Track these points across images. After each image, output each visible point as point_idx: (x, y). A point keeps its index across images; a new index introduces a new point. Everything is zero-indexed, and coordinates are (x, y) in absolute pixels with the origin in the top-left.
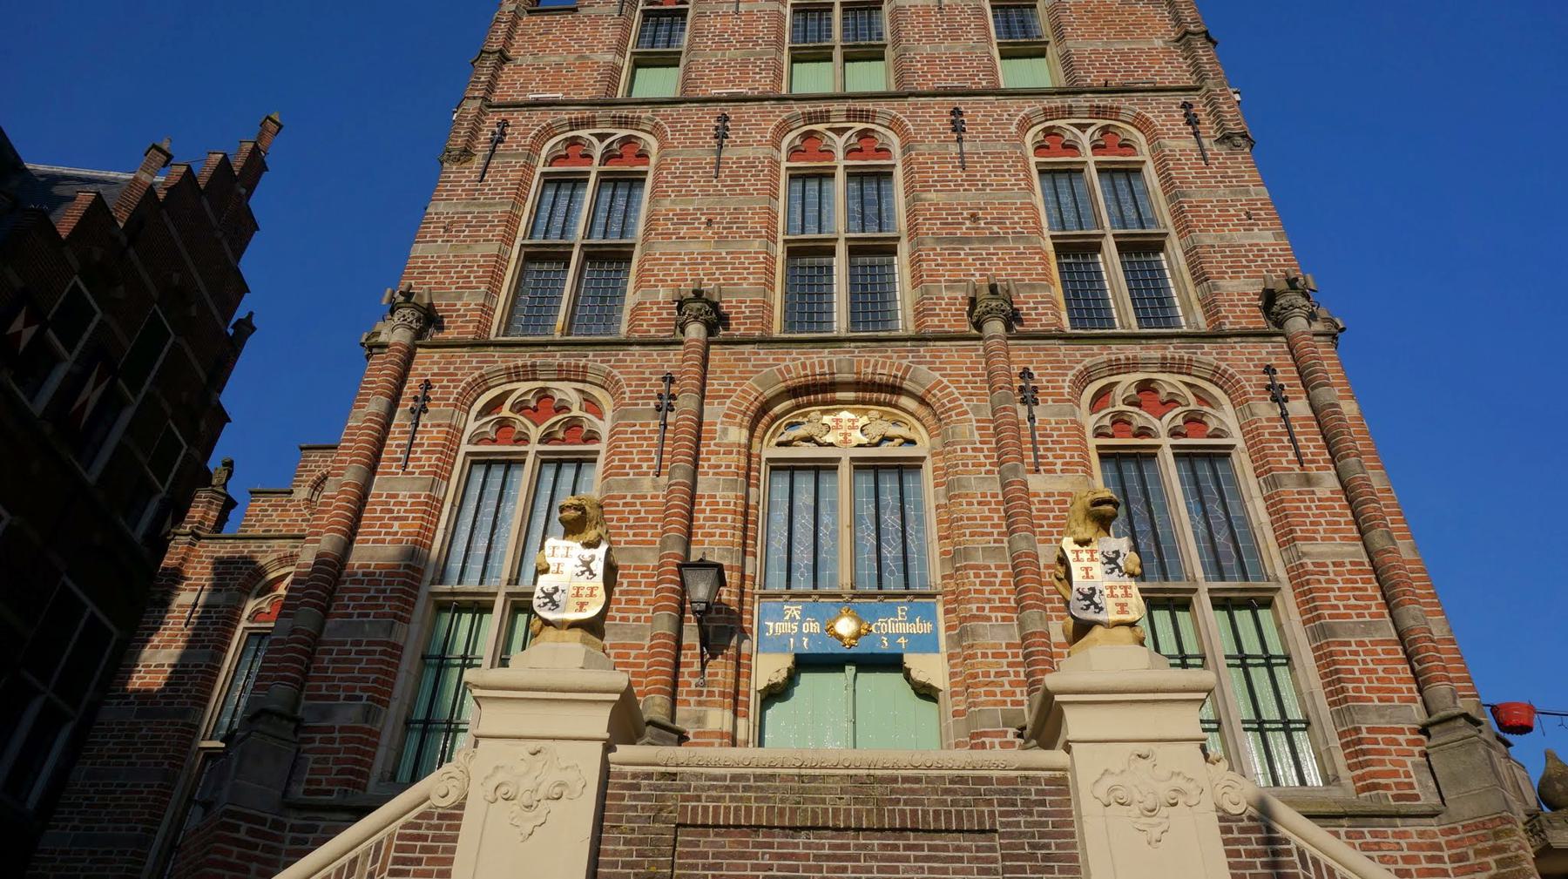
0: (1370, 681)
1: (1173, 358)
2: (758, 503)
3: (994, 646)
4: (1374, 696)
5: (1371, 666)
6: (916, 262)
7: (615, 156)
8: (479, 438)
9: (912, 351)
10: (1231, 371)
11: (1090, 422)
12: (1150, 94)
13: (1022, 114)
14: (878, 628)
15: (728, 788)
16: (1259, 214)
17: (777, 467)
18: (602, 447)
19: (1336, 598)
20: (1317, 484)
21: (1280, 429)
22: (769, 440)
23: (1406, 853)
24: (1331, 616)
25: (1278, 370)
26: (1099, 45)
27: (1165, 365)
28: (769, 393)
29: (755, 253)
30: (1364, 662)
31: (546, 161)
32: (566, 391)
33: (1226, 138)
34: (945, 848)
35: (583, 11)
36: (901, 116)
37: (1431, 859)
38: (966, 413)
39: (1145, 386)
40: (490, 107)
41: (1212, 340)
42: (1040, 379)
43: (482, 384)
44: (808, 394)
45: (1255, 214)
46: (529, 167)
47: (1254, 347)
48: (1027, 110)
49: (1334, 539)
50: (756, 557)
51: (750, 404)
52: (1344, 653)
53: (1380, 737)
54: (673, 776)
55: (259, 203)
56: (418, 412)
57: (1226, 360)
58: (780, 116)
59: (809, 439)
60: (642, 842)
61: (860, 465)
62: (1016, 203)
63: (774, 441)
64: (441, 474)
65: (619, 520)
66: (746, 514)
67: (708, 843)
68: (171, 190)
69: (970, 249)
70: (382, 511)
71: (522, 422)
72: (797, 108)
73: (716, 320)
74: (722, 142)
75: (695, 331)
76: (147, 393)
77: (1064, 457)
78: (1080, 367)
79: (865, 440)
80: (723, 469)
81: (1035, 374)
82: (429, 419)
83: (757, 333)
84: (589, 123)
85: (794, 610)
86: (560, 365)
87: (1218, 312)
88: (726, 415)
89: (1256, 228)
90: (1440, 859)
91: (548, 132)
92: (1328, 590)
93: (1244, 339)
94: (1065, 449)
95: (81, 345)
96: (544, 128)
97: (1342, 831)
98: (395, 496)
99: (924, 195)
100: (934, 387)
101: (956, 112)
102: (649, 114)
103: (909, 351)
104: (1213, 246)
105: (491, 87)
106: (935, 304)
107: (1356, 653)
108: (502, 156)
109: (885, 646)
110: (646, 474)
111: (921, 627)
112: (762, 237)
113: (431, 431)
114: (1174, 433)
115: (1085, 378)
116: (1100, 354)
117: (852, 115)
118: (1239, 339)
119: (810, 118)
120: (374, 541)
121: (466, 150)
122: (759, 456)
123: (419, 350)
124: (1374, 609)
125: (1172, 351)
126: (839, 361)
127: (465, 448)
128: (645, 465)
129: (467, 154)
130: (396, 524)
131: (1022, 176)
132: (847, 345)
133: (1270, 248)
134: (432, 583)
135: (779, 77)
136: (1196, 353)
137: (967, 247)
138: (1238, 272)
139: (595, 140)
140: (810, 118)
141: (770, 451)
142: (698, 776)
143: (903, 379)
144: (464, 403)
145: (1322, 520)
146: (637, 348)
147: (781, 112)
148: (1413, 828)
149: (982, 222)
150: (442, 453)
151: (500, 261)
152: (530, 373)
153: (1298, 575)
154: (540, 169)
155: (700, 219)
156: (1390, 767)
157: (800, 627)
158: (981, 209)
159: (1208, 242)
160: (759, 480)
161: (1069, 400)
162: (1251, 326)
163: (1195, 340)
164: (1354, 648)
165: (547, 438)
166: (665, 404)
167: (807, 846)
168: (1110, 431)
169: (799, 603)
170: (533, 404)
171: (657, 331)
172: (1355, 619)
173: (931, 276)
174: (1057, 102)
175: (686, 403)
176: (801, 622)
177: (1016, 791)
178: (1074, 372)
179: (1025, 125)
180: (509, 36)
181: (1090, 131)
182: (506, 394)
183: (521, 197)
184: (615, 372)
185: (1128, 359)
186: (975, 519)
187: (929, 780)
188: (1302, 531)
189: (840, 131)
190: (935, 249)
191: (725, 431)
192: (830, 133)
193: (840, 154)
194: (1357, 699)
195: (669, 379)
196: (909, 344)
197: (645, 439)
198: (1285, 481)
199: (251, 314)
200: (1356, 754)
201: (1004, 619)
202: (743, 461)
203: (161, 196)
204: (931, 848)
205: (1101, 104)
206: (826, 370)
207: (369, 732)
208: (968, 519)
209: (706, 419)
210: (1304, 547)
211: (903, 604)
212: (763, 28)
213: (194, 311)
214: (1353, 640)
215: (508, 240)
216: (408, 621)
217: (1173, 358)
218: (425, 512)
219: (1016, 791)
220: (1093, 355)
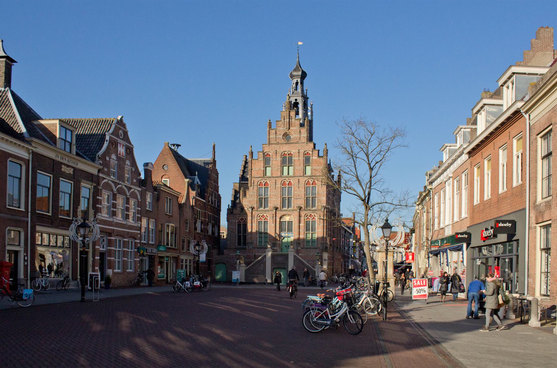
6: (293, 201)
11: (306, 218)
27: (312, 213)
32: (265, 215)
35: (259, 159)
39: (310, 215)
43: (258, 215)
46: (257, 187)
51: (279, 217)
61: (288, 222)
64: (257, 223)
72: (283, 179)
73: (276, 209)
75: (274, 210)
99: (295, 192)
101: (299, 180)
111: (292, 235)
114: (312, 219)
115: (306, 214)
117: (288, 179)
119: (284, 180)
140: (284, 180)
141: (281, 220)
152: (262, 213)
165: (264, 219)
179: (305, 182)
183: (257, 191)
215: (257, 198)
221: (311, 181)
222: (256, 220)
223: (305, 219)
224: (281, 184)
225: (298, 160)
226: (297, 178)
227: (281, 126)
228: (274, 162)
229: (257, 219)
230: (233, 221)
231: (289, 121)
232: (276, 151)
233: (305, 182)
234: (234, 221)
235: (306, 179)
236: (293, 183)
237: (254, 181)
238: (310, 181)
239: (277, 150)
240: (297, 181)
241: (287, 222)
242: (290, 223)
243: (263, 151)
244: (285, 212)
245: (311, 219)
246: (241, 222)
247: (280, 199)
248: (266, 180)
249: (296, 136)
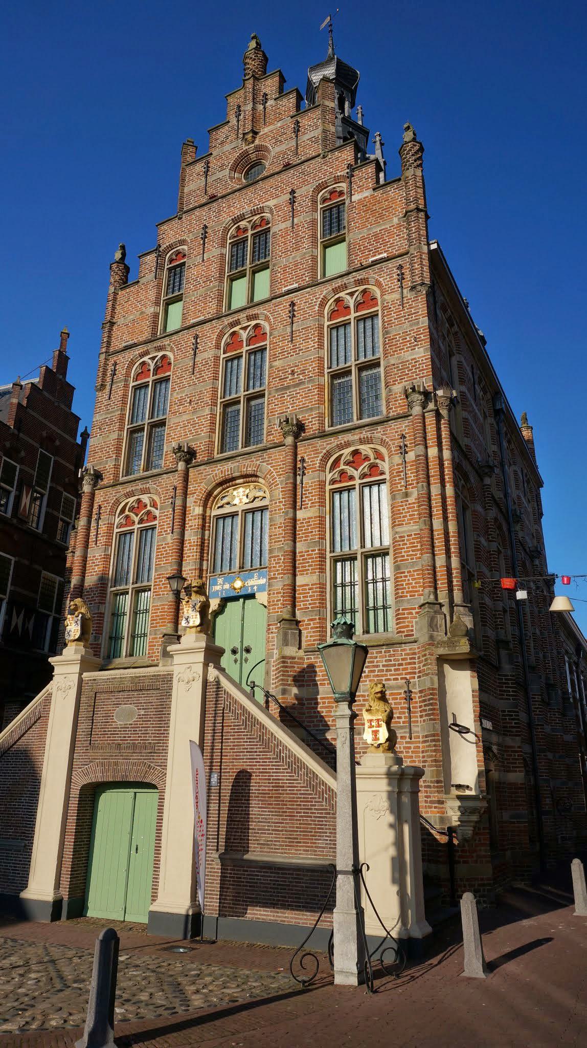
0: (409, 588)
1: (364, 438)
2: (209, 537)
3: (277, 590)
4: (408, 595)
5: (411, 581)
7: (159, 367)
8: (120, 525)
9: (261, 456)
10: (387, 440)
11: (329, 477)
12: (384, 263)
13: (322, 296)
14: (247, 584)
15: (106, 682)
16: (420, 337)
17: (218, 518)
19: (405, 552)
20: (410, 496)
21: (401, 469)
22: (215, 506)
23: (403, 657)
24: (401, 561)
25: (407, 436)
26: (365, 232)
27: (362, 441)
28: (209, 488)
29: (207, 415)
30: (409, 580)
31: (134, 378)
33: (413, 288)
34: (150, 694)
35: (142, 281)
36: (268, 313)
37: (411, 659)
38: (278, 484)
39: (356, 453)
40: (109, 355)
41: (382, 424)
43: (118, 502)
44: (226, 483)
45: (419, 338)
46: (126, 386)
47: (400, 424)
48: (325, 292)
49: (410, 523)
50: (208, 561)
52: (401, 577)
53: (406, 612)
54: (94, 680)
55: (70, 379)
57: (386, 434)
58: (219, 328)
59: (228, 503)
60: (88, 697)
61: (246, 512)
62: (311, 359)
63: (217, 506)
64: (108, 544)
65: (161, 555)
66: (203, 543)
67: (103, 696)
68: (29, 398)
69: (290, 392)
70: (92, 563)
74: (196, 351)
75: (181, 466)
76: (50, 487)
77: (312, 500)
78: (324, 451)
79: (247, 501)
80: (193, 527)
81: (306, 458)
82: (102, 522)
83: (206, 459)
84: (146, 353)
85: (220, 581)
86: (141, 489)
87: (389, 406)
88: (195, 502)
89: (416, 347)
90: (414, 658)
91: (132, 363)
92: (402, 549)
93: (396, 421)
94: (312, 496)
95: (16, 482)
96: (130, 362)
97: (383, 650)
98: (94, 557)
100: (267, 474)
102: (168, 342)
103: (259, 457)
104: (394, 365)
105: (109, 343)
106: (272, 428)
107: (406, 576)
108: (116, 382)
109: (250, 591)
110: (169, 534)
112: (209, 405)
113: (103, 528)
114: (363, 476)
115: (328, 455)
116: (334, 442)
117: (249, 318)
118: (394, 421)
119: (232, 325)
120: (91, 575)
121: (102, 385)
122: (210, 516)
123: (96, 491)
124: (418, 556)
125: (365, 434)
126: (234, 467)
127: (116, 530)
128: (168, 529)
129: (103, 386)
130: (96, 567)
131: (316, 340)
132: (237, 458)
133: (420, 359)
134: (111, 587)
135: (220, 301)
136: (374, 433)
137: (288, 392)
138: (402, 379)
139: (150, 361)
140: (232, 325)
141: (216, 512)
142: (100, 679)
143: (257, 471)
144: (112, 512)
145: (408, 514)
146: (165, 475)
147: (218, 325)
148: (407, 647)
149: (296, 374)
150: (107, 536)
151: (119, 439)
153: (394, 541)
154: (132, 384)
155: (187, 401)
156: (407, 624)
157: (222, 587)
158: (296, 366)
159: (392, 362)
160: (210, 526)
161: (318, 470)
162: (401, 412)
163: (375, 426)
164: (406, 574)
165: (141, 521)
167: (122, 695)
168: (338, 479)
169: (222, 577)
170: (136, 506)
171: (172, 465)
172: (410, 561)
173: (272, 412)
174: (339, 282)
176: (224, 584)
177: (165, 678)
178: (322, 454)
179: (322, 305)
180: (114, 308)
181: (355, 296)
182: (127, 504)
184: (158, 488)
185: (345, 442)
186: (276, 535)
187: (148, 676)
188: (398, 521)
189: (245, 328)
190: (275, 396)
191: (194, 509)
192: (241, 331)
194: (402, 597)
196: (260, 453)
197: (168, 518)
198: (397, 496)
199: (86, 427)
200: (398, 619)
201: (282, 577)
202: (200, 522)
203: (24, 403)
204: (147, 694)
205: (360, 278)
206: (229, 473)
207: (97, 644)
208: (274, 535)
209: (188, 505)
210: (398, 529)
211: (255, 572)
212: (214, 269)
213: (57, 443)
214: (406, 571)
216: (105, 603)
217: (364, 438)
218: (104, 561)
219: (165, 678)
220: (331, 444)
221: (351, 294)
222: (103, 528)
223: (322, 484)
224: (218, 347)
226: (285, 301)
227: (227, 137)
229: (111, 526)
231: (254, 109)
233: (322, 305)
235: (325, 290)
236: (268, 329)
238: (348, 297)
240: (285, 314)
241: (238, 520)
244: (230, 465)
247: (207, 411)
248: (160, 349)
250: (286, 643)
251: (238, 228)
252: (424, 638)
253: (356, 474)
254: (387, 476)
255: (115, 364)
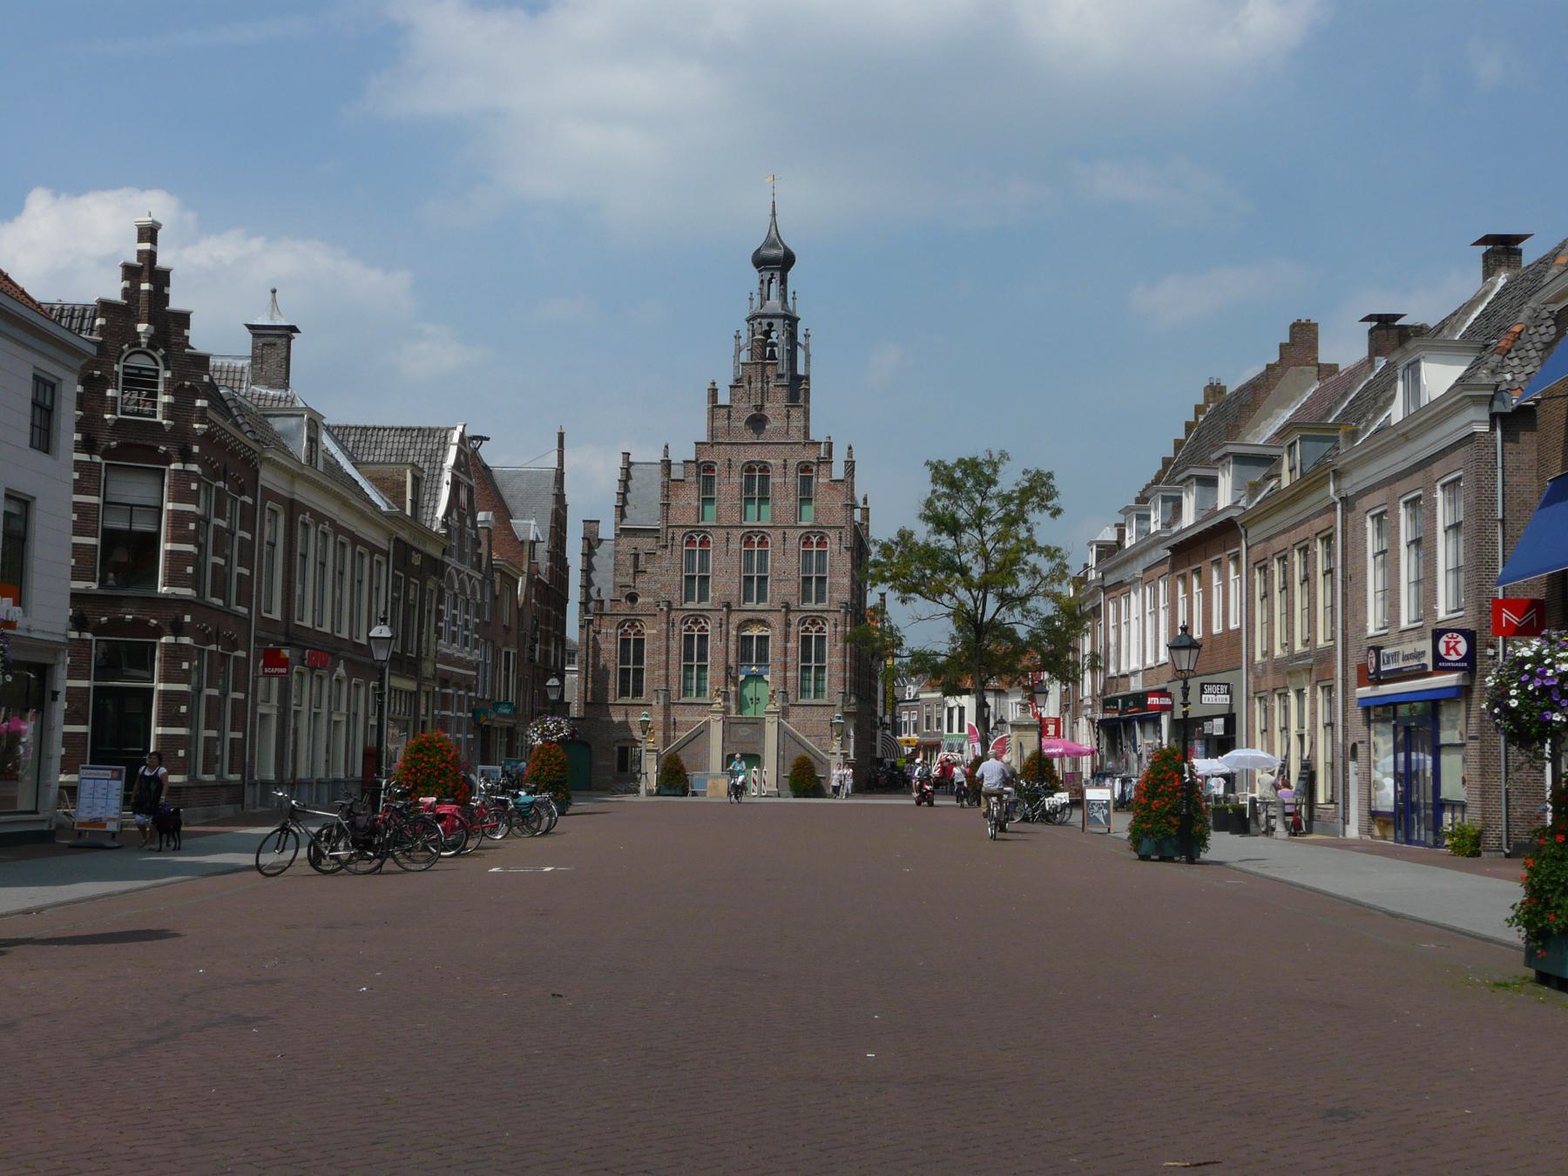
6: (771, 586)
18: (709, 633)
42: (792, 621)
56: (673, 626)
71: (693, 627)
101: (784, 533)
113: (677, 632)
114: (816, 632)
147: (742, 532)
153: (829, 664)
165: (699, 631)
166: (721, 627)
175: (724, 627)
193: (756, 545)
195: (721, 619)
212: (737, 491)
215: (682, 576)
222: (677, 632)
225: (783, 483)
226: (781, 531)
227: (742, 397)
228: (724, 489)
230: (609, 631)
231: (762, 388)
232: (730, 460)
234: (612, 631)
237: (673, 533)
239: (732, 459)
240: (780, 537)
242: (763, 640)
243: (697, 459)
245: (814, 630)
246: (630, 634)
247: (737, 581)
249: (779, 424)
250: (783, 701)
251: (750, 467)
252: (839, 704)
253: (814, 630)
254: (827, 634)
255: (673, 533)
